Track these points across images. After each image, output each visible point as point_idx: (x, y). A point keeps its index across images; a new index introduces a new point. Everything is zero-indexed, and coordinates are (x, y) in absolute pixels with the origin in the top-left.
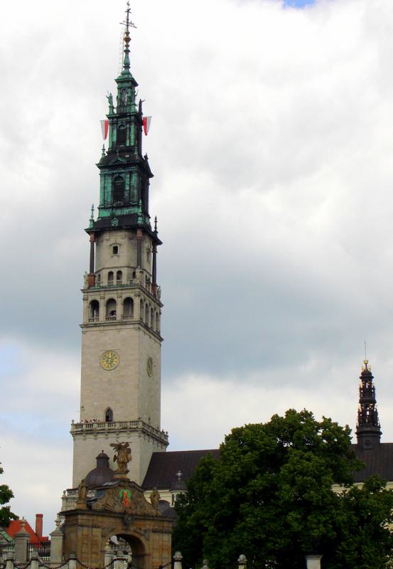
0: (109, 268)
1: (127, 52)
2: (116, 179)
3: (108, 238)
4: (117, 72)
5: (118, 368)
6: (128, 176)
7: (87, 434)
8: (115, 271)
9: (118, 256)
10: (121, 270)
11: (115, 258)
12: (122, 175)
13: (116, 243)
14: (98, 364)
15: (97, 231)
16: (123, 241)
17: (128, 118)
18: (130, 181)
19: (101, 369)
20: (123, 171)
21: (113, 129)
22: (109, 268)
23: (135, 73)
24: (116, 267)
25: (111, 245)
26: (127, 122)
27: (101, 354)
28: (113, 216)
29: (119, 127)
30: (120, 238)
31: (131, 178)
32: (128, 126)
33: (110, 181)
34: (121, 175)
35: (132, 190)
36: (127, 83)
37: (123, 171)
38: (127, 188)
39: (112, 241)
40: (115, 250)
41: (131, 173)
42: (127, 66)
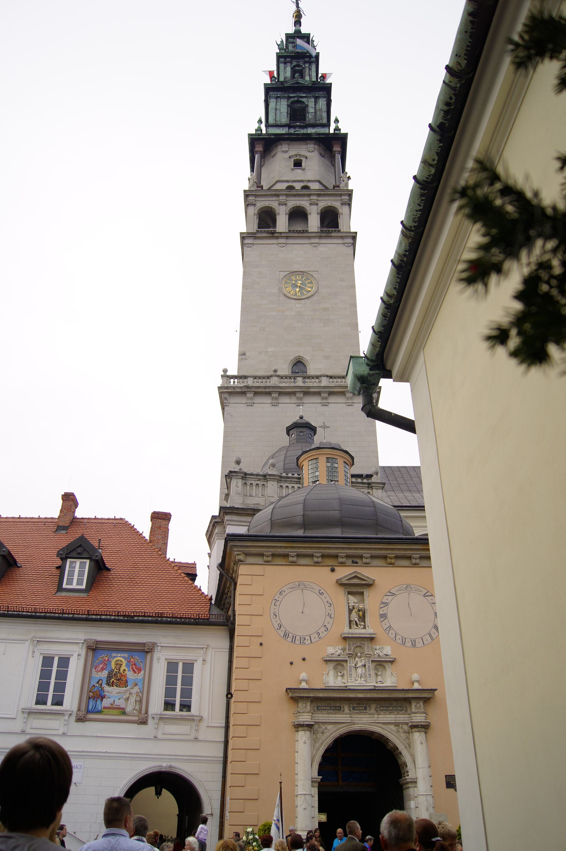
0: (288, 181)
2: (293, 103)
3: (287, 149)
5: (315, 298)
6: (313, 100)
7: (256, 393)
9: (304, 170)
11: (298, 171)
12: (304, 100)
14: (275, 290)
16: (313, 154)
17: (307, 59)
18: (315, 105)
19: (282, 298)
20: (304, 95)
21: (285, 68)
22: (288, 181)
26: (305, 62)
27: (282, 276)
29: (295, 66)
31: (316, 102)
32: (307, 65)
33: (286, 103)
34: (301, 99)
35: (318, 113)
37: (304, 95)
38: (311, 110)
40: (298, 164)
41: (316, 98)
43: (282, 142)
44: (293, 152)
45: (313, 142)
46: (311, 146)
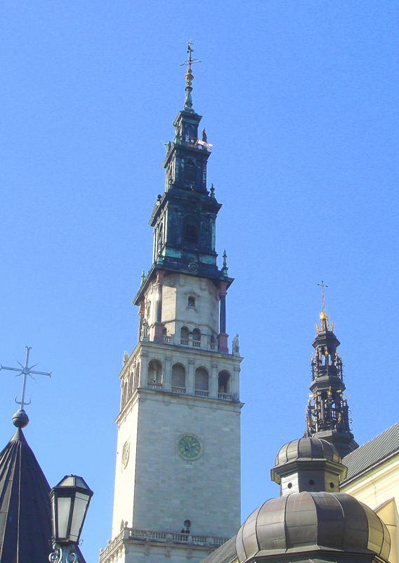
1: (190, 89)
4: (183, 107)
8: (191, 328)
9: (196, 310)
10: (200, 328)
11: (191, 311)
13: (194, 293)
15: (165, 272)
23: (197, 110)
24: (195, 324)
25: (186, 294)
28: (184, 261)
30: (198, 287)
36: (190, 120)
39: (187, 288)
40: (192, 301)
42: (189, 103)
43: (181, 275)
44: (187, 288)
45: (205, 280)
46: (204, 283)
